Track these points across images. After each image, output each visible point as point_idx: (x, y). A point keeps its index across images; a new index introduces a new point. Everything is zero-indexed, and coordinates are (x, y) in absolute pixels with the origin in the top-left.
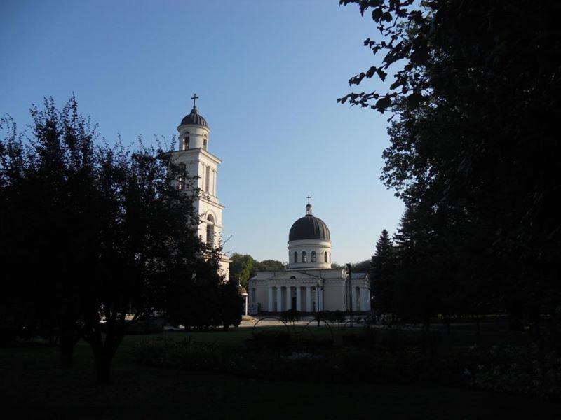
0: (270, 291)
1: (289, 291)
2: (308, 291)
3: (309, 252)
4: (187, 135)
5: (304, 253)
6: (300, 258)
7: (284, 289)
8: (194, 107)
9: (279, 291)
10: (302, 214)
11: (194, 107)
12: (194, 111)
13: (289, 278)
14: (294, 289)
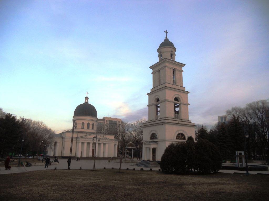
0: (80, 144)
1: (91, 145)
2: (102, 145)
3: (91, 123)
5: (88, 124)
6: (86, 126)
7: (88, 144)
8: (166, 37)
9: (86, 144)
10: (83, 102)
11: (166, 37)
12: (166, 40)
13: (93, 137)
14: (94, 144)
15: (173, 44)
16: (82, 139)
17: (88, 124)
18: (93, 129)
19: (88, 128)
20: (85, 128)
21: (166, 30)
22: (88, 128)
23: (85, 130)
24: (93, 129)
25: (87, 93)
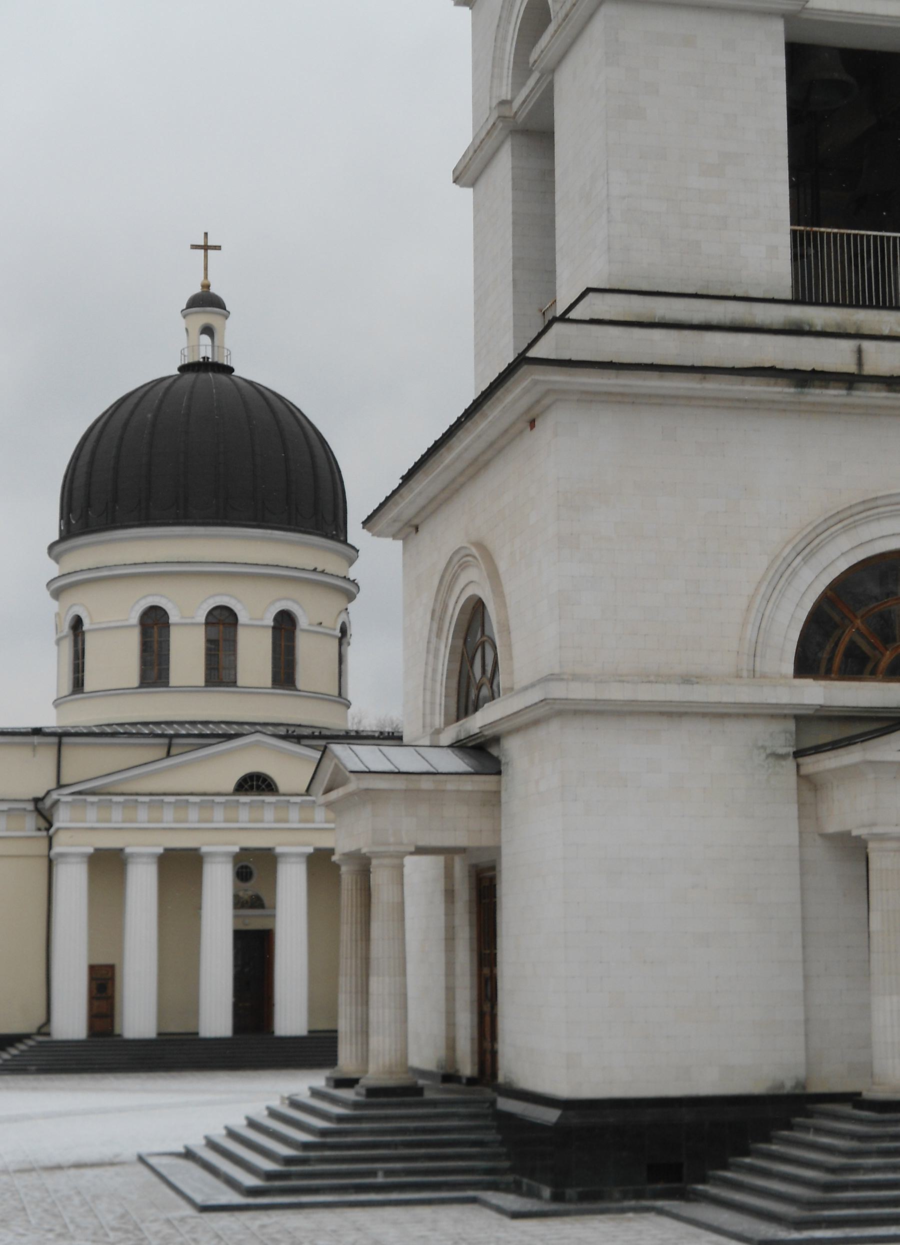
13: (231, 786)
16: (91, 816)
20: (175, 678)
25: (206, 248)
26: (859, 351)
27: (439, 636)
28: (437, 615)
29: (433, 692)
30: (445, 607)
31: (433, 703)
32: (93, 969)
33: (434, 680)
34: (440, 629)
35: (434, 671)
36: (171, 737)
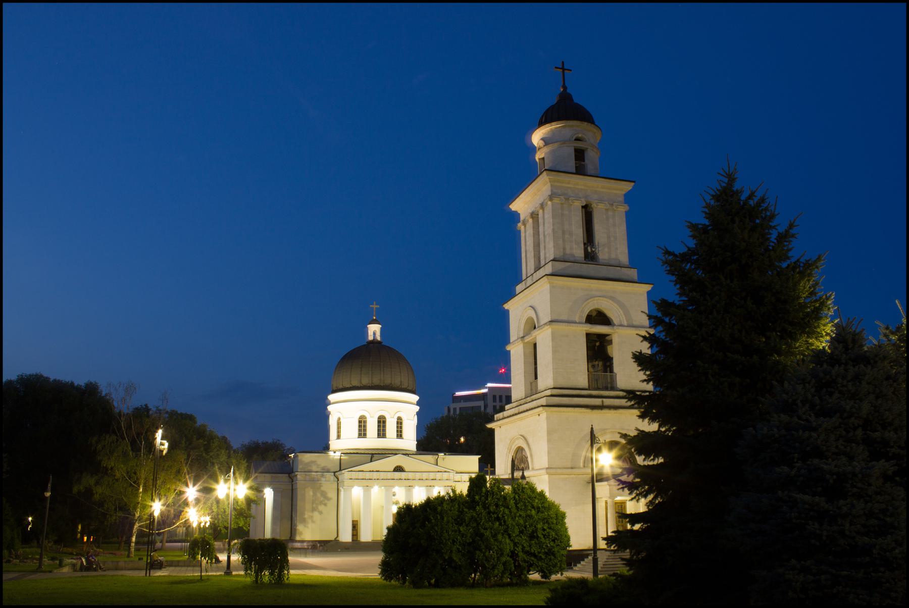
4: (580, 145)
5: (382, 422)
6: (372, 427)
8: (565, 88)
11: (565, 88)
12: (565, 97)
15: (584, 108)
17: (382, 422)
18: (400, 435)
19: (381, 433)
21: (563, 62)
22: (381, 433)
23: (372, 442)
24: (400, 435)
26: (603, 401)
27: (509, 453)
28: (509, 449)
29: (507, 465)
30: (511, 447)
31: (507, 467)
32: (353, 521)
33: (508, 463)
34: (510, 451)
35: (508, 460)
36: (372, 454)
